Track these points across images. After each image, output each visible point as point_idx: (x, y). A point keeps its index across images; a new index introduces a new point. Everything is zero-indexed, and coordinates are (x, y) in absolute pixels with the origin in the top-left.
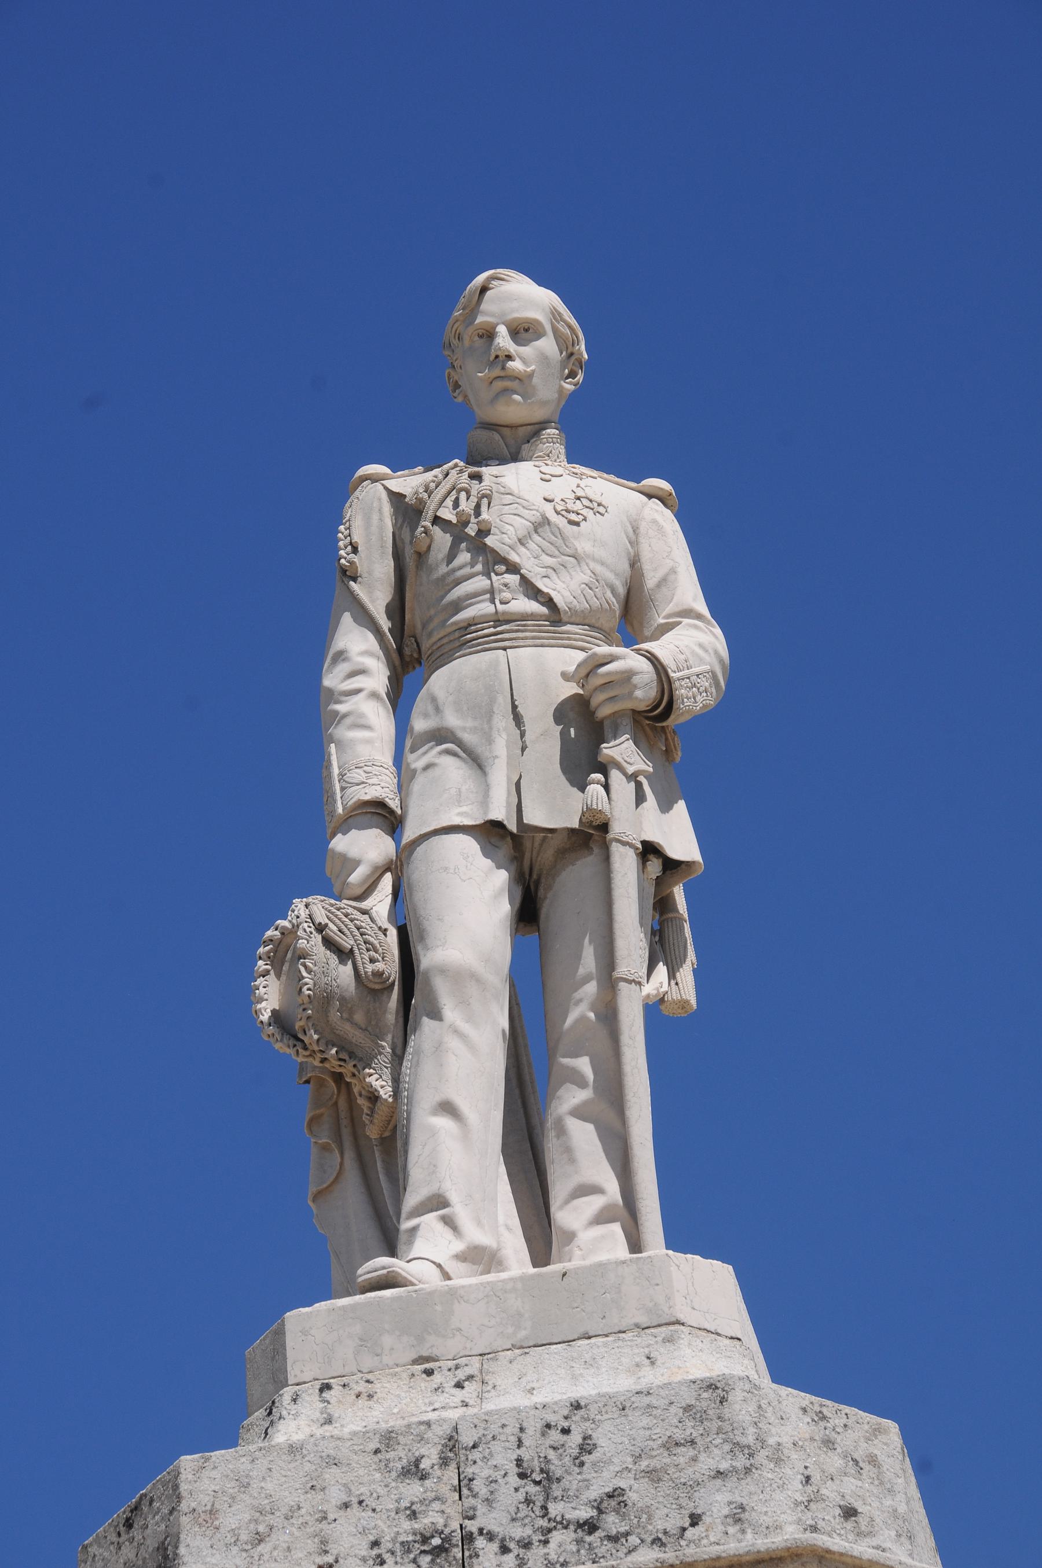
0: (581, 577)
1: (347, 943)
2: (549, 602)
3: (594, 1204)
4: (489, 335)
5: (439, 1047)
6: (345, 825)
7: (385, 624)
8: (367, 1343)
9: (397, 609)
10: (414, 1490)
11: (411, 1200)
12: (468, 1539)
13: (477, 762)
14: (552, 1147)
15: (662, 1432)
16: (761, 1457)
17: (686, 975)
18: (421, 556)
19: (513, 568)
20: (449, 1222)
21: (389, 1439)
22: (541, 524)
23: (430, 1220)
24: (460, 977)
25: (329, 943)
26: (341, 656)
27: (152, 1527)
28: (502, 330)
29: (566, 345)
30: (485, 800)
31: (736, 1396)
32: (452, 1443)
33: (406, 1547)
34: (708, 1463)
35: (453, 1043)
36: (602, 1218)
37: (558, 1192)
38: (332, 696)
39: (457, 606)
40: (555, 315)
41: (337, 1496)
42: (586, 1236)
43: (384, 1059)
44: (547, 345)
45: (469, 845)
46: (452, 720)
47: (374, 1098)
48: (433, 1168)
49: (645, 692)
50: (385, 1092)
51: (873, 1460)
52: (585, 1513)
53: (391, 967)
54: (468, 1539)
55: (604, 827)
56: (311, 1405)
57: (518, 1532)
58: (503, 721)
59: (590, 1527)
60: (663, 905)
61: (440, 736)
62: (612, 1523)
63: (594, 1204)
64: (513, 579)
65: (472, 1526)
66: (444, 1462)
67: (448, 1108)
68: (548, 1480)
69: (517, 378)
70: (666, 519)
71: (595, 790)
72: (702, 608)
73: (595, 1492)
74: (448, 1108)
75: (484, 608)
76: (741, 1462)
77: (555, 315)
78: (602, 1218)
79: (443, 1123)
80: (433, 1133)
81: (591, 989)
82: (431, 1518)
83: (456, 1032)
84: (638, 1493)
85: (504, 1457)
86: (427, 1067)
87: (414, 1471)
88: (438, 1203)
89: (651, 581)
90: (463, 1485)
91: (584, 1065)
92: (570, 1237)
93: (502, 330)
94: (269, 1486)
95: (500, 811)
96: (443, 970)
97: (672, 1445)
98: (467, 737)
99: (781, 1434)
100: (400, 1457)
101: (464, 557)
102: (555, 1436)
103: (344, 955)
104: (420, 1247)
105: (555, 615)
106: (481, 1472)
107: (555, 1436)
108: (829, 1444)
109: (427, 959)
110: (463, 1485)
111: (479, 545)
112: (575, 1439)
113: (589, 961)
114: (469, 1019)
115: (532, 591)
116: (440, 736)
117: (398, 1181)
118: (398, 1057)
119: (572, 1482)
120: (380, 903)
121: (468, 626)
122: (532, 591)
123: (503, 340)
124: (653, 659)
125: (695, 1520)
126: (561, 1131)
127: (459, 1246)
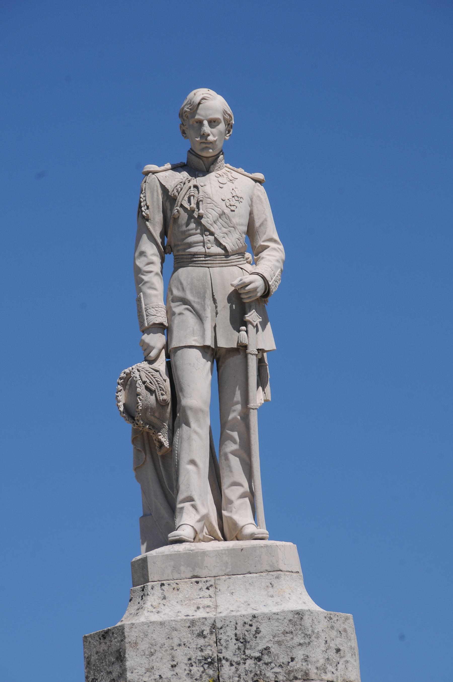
1: (153, 387)
2: (224, 248)
3: (239, 490)
4: (200, 123)
5: (189, 438)
7: (159, 241)
8: (176, 569)
9: (164, 233)
10: (201, 642)
11: (181, 497)
12: (220, 660)
14: (222, 464)
16: (313, 638)
18: (176, 220)
19: (212, 234)
20: (194, 507)
21: (193, 623)
22: (222, 214)
24: (196, 411)
25: (147, 388)
26: (142, 254)
27: (115, 644)
29: (229, 125)
30: (203, 336)
31: (306, 617)
32: (214, 626)
33: (200, 661)
35: (194, 436)
36: (242, 496)
39: (190, 245)
41: (176, 641)
42: (237, 503)
44: (222, 127)
45: (197, 353)
46: (190, 297)
47: (161, 445)
52: (257, 654)
53: (167, 397)
54: (220, 660)
56: (157, 592)
57: (236, 659)
58: (209, 302)
59: (259, 659)
61: (185, 301)
62: (266, 658)
63: (239, 490)
64: (211, 238)
65: (221, 656)
66: (211, 633)
67: (193, 462)
69: (211, 143)
70: (260, 190)
72: (276, 237)
73: (260, 647)
74: (193, 462)
76: (307, 641)
78: (242, 496)
79: (191, 467)
80: (188, 472)
82: (207, 652)
83: (195, 432)
84: (274, 649)
85: (231, 633)
86: (185, 445)
87: (201, 635)
88: (190, 499)
89: (257, 224)
91: (235, 435)
93: (206, 123)
94: (154, 636)
95: (209, 342)
96: (191, 408)
97: (285, 633)
98: (195, 305)
99: (319, 628)
100: (197, 630)
101: (192, 225)
102: (247, 627)
103: (152, 392)
105: (227, 254)
106: (223, 637)
107: (247, 627)
112: (254, 628)
113: (238, 396)
115: (219, 244)
116: (185, 301)
119: (253, 643)
120: (161, 364)
121: (194, 255)
122: (219, 244)
123: (206, 128)
125: (293, 659)
126: (227, 459)
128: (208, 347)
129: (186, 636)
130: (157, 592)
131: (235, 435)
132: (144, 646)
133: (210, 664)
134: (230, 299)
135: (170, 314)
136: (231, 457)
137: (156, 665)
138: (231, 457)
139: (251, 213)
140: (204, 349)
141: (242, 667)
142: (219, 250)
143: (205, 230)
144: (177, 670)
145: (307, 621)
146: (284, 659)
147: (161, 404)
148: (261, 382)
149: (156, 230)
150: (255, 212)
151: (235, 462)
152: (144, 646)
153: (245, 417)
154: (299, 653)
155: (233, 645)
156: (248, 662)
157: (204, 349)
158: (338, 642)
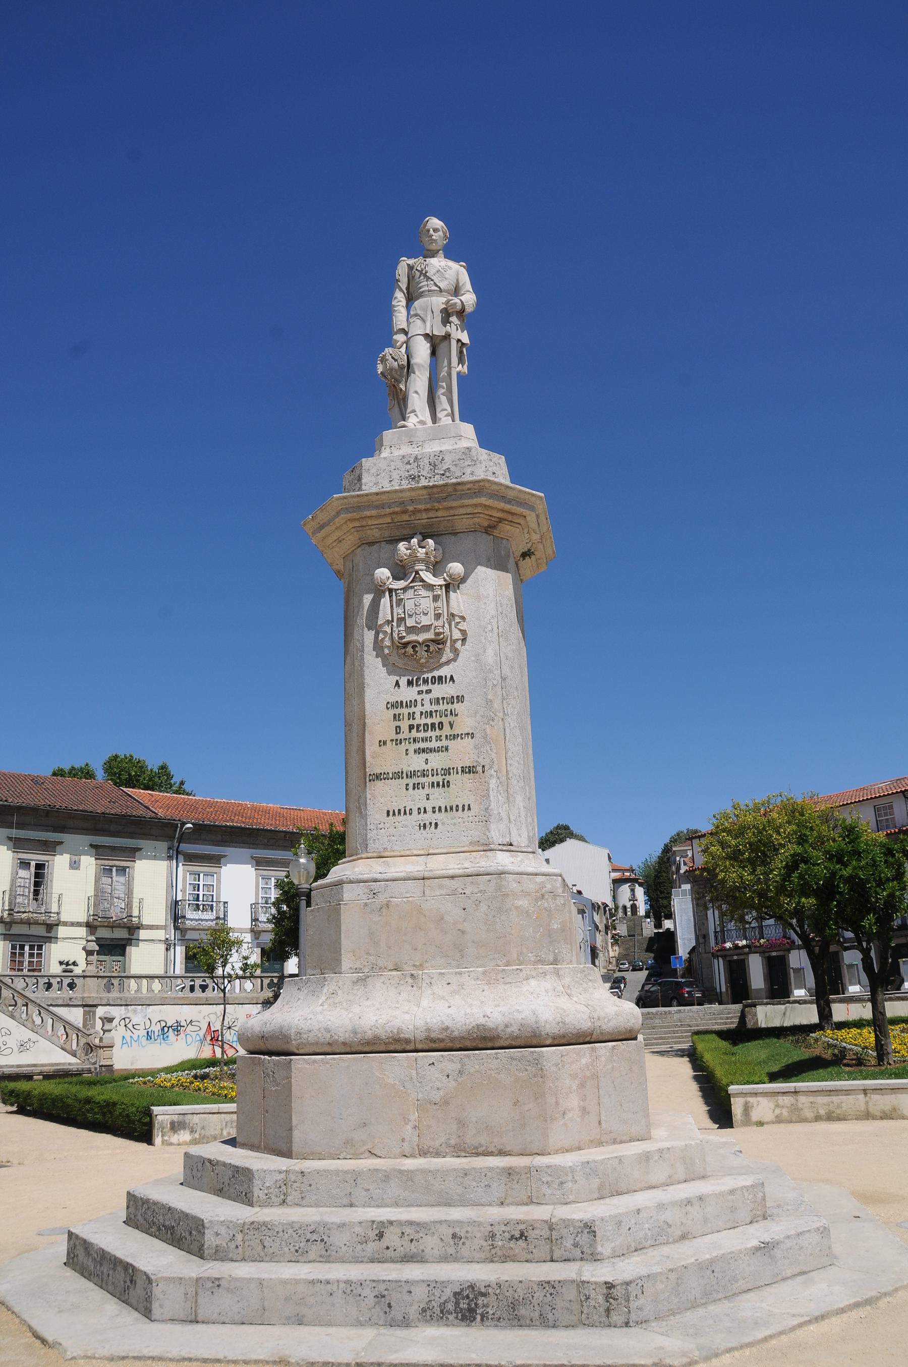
0: (446, 282)
1: (396, 358)
2: (440, 288)
3: (446, 412)
4: (429, 231)
5: (415, 379)
6: (396, 333)
7: (405, 292)
8: (399, 438)
9: (408, 288)
10: (408, 467)
11: (408, 411)
12: (419, 476)
13: (424, 321)
14: (437, 401)
15: (458, 457)
16: (477, 462)
17: (465, 367)
18: (413, 277)
19: (432, 280)
20: (415, 415)
21: (404, 457)
22: (438, 271)
23: (412, 414)
24: (419, 365)
25: (392, 358)
27: (357, 472)
28: (431, 230)
30: (425, 329)
31: (473, 450)
32: (416, 458)
33: (407, 478)
34: (467, 463)
35: (418, 379)
36: (447, 415)
37: (438, 410)
38: (394, 306)
39: (420, 288)
40: (442, 227)
41: (393, 467)
42: (443, 419)
43: (403, 382)
44: (441, 233)
46: (419, 312)
47: (401, 390)
48: (413, 405)
49: (459, 307)
50: (404, 389)
51: (499, 464)
52: (442, 472)
53: (405, 363)
54: (419, 476)
55: (450, 335)
56: (388, 450)
57: (429, 475)
58: (429, 312)
59: (443, 475)
60: (461, 352)
61: (416, 315)
62: (447, 474)
63: (446, 412)
64: (432, 282)
65: (420, 474)
66: (415, 462)
67: (416, 392)
68: (435, 465)
69: (434, 240)
70: (464, 271)
71: (448, 327)
72: (471, 290)
73: (444, 469)
74: (416, 392)
75: (426, 288)
76: (473, 463)
77: (442, 227)
78: (447, 415)
79: (415, 395)
80: (413, 397)
81: (446, 368)
82: (412, 472)
84: (453, 468)
85: (427, 461)
86: (412, 383)
87: (408, 463)
88: (414, 411)
89: (461, 284)
90: (418, 466)
91: (444, 384)
92: (440, 419)
93: (431, 230)
95: (428, 332)
96: (416, 364)
97: (459, 459)
98: (422, 316)
99: (481, 458)
100: (406, 460)
101: (422, 277)
102: (437, 457)
103: (396, 360)
104: (410, 420)
105: (441, 290)
107: (437, 457)
108: (491, 460)
109: (412, 362)
110: (418, 466)
111: (425, 275)
112: (441, 458)
113: (446, 361)
114: (421, 374)
115: (437, 286)
116: (416, 315)
117: (406, 407)
118: (406, 382)
119: (440, 466)
120: (403, 350)
121: (422, 292)
122: (437, 286)
123: (431, 232)
124: (461, 300)
125: (464, 474)
126: (439, 398)
127: (418, 420)
128: (428, 334)
129: (399, 464)
130: (388, 450)
131: (444, 384)
132: (373, 471)
133: (413, 479)
134: (441, 312)
135: (409, 323)
136: (441, 396)
137: (380, 481)
138: (441, 396)
139: (457, 280)
140: (426, 336)
141: (433, 479)
142: (436, 288)
143: (428, 278)
144: (393, 483)
145: (474, 453)
146: (458, 474)
147: (401, 367)
148: (461, 361)
149: (404, 286)
150: (460, 278)
151: (444, 399)
152: (373, 471)
153: (449, 374)
154: (468, 471)
155: (427, 468)
156: (436, 476)
157: (426, 336)
158: (494, 469)
